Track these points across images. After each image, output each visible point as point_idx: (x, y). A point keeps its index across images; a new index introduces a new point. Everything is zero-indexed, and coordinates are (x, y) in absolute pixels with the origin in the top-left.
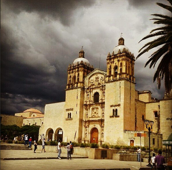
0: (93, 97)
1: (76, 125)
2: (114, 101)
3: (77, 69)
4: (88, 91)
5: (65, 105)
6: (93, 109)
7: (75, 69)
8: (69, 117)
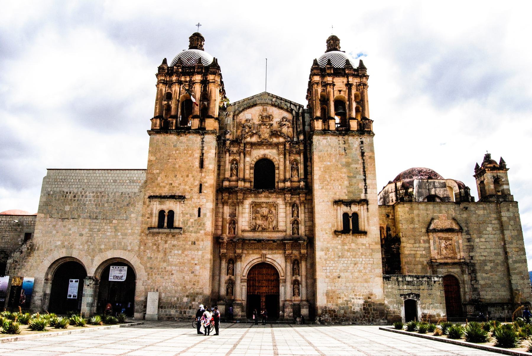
0: (252, 171)
1: (200, 253)
2: (345, 191)
3: (198, 78)
4: (235, 149)
5: (146, 182)
6: (255, 206)
7: (191, 74)
8: (166, 224)
